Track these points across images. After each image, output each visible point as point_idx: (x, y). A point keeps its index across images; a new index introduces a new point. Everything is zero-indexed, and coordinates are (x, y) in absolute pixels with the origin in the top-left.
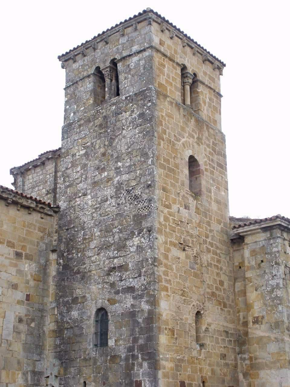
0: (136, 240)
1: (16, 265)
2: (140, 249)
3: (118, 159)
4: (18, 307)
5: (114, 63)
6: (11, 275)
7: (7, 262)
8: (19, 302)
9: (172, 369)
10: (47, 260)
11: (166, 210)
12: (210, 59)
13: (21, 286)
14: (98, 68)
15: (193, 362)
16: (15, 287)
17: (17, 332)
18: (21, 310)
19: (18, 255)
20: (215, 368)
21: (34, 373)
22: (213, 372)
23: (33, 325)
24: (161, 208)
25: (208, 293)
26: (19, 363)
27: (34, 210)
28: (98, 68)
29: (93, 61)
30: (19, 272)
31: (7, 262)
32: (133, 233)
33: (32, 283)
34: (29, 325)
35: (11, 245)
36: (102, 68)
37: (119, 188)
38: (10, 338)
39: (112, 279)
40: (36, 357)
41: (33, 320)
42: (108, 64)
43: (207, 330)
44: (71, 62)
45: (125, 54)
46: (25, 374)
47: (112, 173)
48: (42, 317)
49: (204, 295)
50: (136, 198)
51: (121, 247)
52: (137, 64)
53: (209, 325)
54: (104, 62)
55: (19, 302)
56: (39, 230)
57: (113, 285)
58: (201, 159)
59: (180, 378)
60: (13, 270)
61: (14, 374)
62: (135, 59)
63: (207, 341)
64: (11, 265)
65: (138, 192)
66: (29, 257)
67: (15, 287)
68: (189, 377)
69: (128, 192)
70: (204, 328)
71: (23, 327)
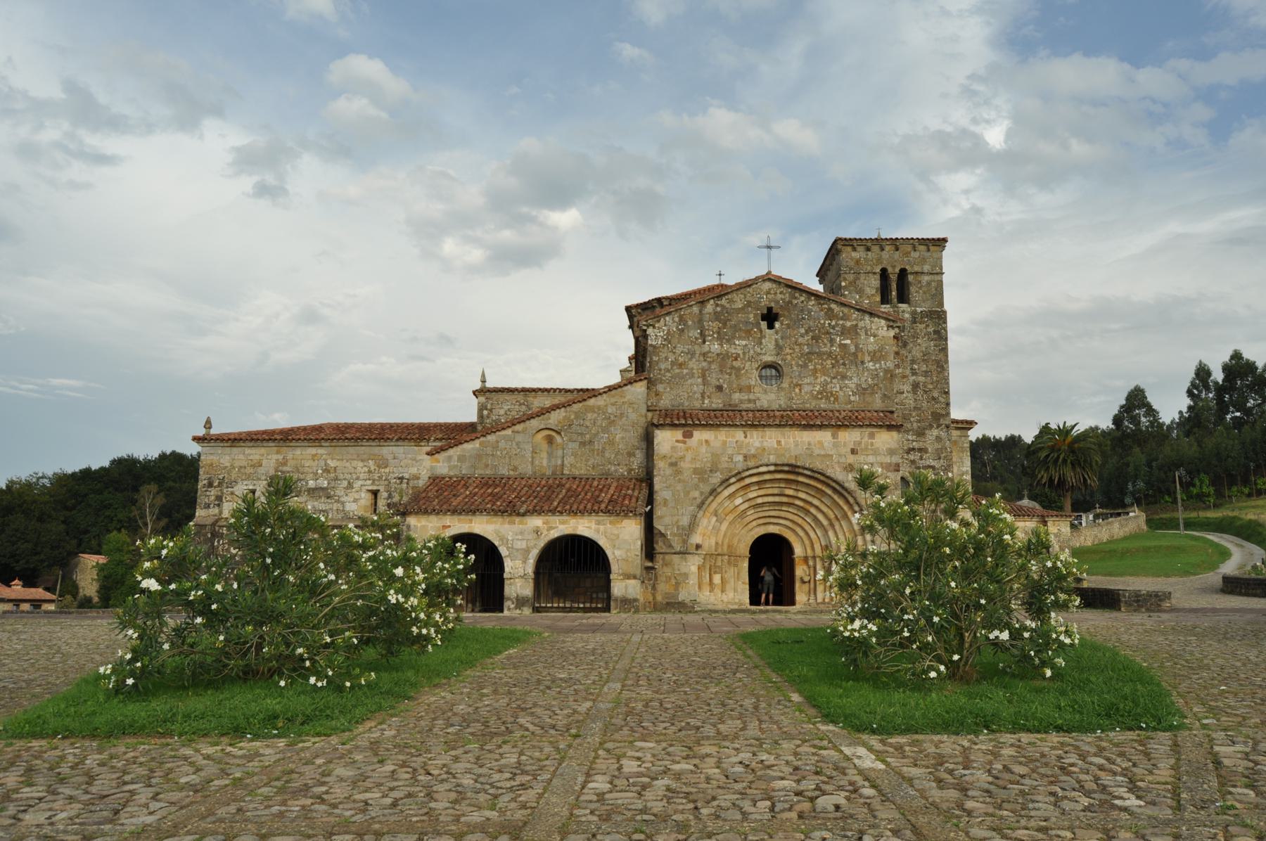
0: (935, 432)
2: (938, 439)
3: (913, 362)
5: (903, 273)
14: (884, 271)
28: (884, 271)
29: (879, 260)
32: (931, 427)
36: (890, 270)
37: (915, 386)
39: (912, 457)
42: (897, 270)
44: (849, 249)
45: (916, 269)
47: (908, 372)
50: (934, 399)
51: (920, 433)
52: (929, 283)
54: (894, 267)
57: (913, 462)
62: (926, 278)
65: (936, 394)
69: (926, 392)
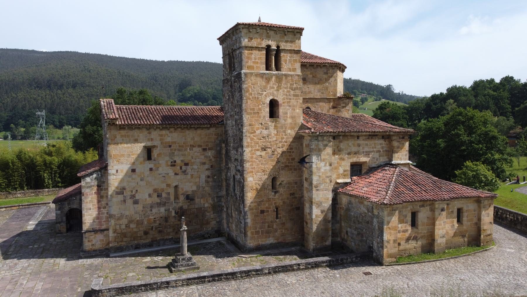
1: (203, 154)
4: (207, 171)
6: (202, 159)
7: (199, 154)
8: (207, 170)
9: (255, 206)
10: (221, 147)
11: (252, 135)
12: (290, 30)
13: (207, 162)
15: (270, 201)
16: (204, 164)
17: (207, 182)
18: (208, 173)
19: (204, 150)
20: (286, 200)
21: (217, 197)
22: (284, 202)
23: (215, 177)
24: (248, 135)
25: (282, 167)
26: (209, 194)
27: (210, 127)
30: (206, 157)
31: (199, 154)
33: (213, 160)
34: (213, 178)
35: (199, 146)
38: (204, 185)
40: (218, 190)
41: (215, 176)
43: (280, 184)
46: (213, 199)
48: (221, 173)
49: (279, 168)
53: (283, 181)
55: (207, 170)
56: (215, 135)
58: (280, 99)
59: (260, 209)
60: (203, 157)
61: (207, 199)
63: (281, 190)
64: (201, 155)
66: (210, 149)
67: (204, 164)
68: (266, 208)
70: (278, 183)
71: (210, 180)
